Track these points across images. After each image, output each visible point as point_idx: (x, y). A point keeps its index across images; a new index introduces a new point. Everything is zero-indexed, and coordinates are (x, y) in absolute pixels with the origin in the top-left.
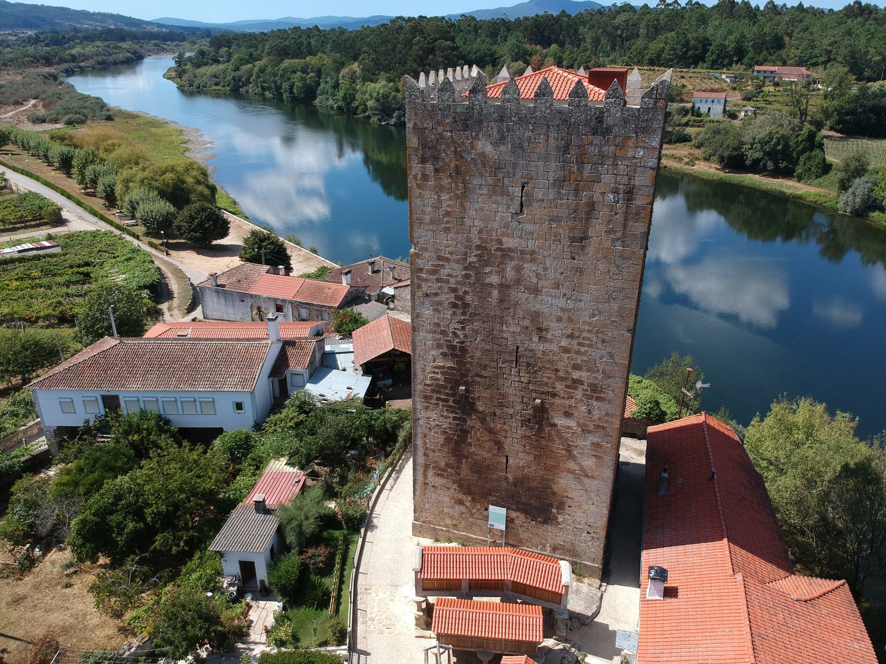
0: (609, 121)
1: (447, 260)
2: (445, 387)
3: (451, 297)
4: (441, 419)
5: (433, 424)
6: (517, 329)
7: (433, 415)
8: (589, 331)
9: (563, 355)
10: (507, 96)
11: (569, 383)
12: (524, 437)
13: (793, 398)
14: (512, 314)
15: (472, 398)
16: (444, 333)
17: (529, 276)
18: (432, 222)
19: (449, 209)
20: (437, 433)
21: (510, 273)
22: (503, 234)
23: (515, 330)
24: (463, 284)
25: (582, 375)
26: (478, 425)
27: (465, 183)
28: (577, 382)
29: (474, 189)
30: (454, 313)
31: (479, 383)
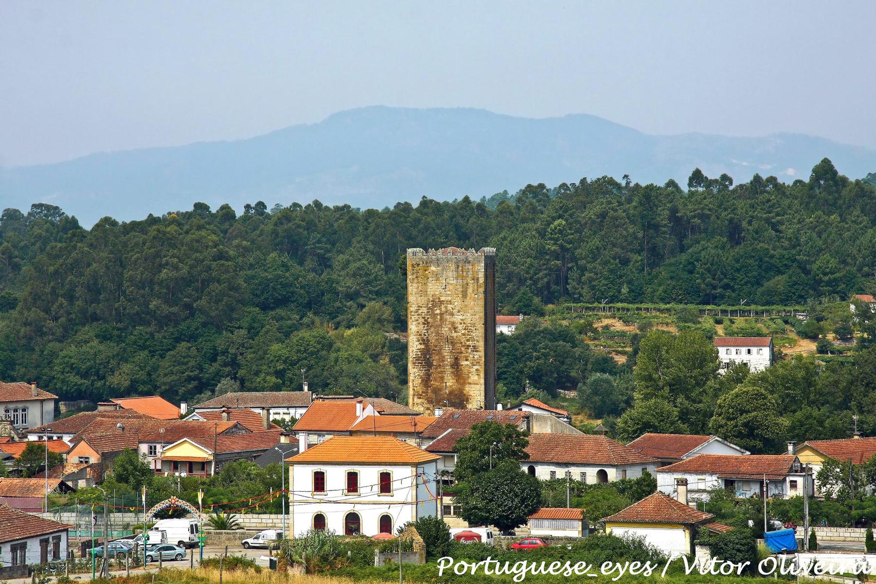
13: (608, 415)
16: (420, 335)
21: (443, 309)
25: (470, 343)
28: (469, 346)
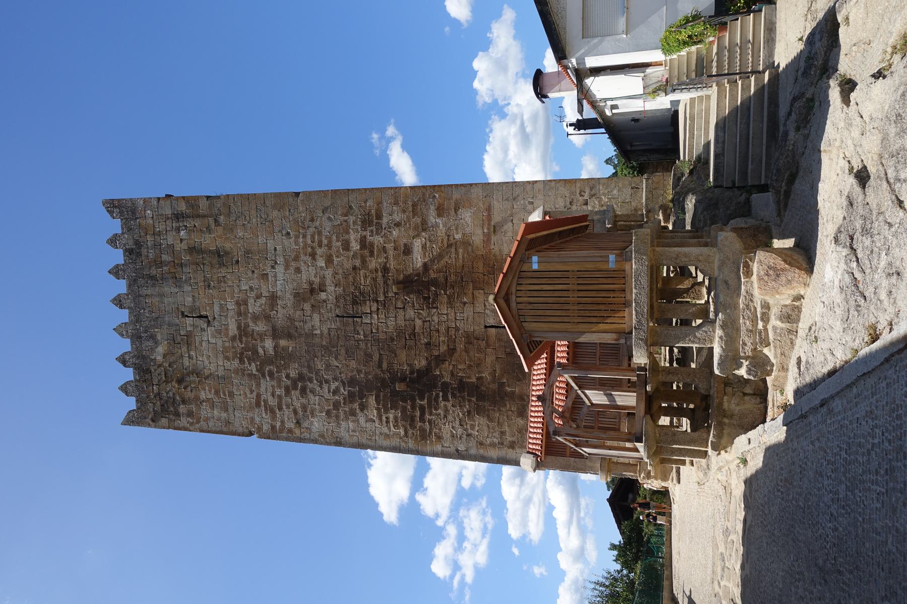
0: (131, 244)
1: (259, 396)
2: (404, 410)
3: (295, 394)
4: (450, 418)
5: (460, 431)
6: (316, 317)
7: (446, 430)
8: (304, 236)
10: (124, 333)
12: (450, 304)
14: (301, 324)
15: (412, 372)
17: (260, 306)
18: (226, 410)
19: (213, 391)
22: (227, 335)
23: (318, 320)
24: (279, 380)
25: (354, 239)
26: (447, 366)
27: (188, 374)
28: (363, 242)
29: (194, 365)
30: (313, 391)
31: (390, 364)
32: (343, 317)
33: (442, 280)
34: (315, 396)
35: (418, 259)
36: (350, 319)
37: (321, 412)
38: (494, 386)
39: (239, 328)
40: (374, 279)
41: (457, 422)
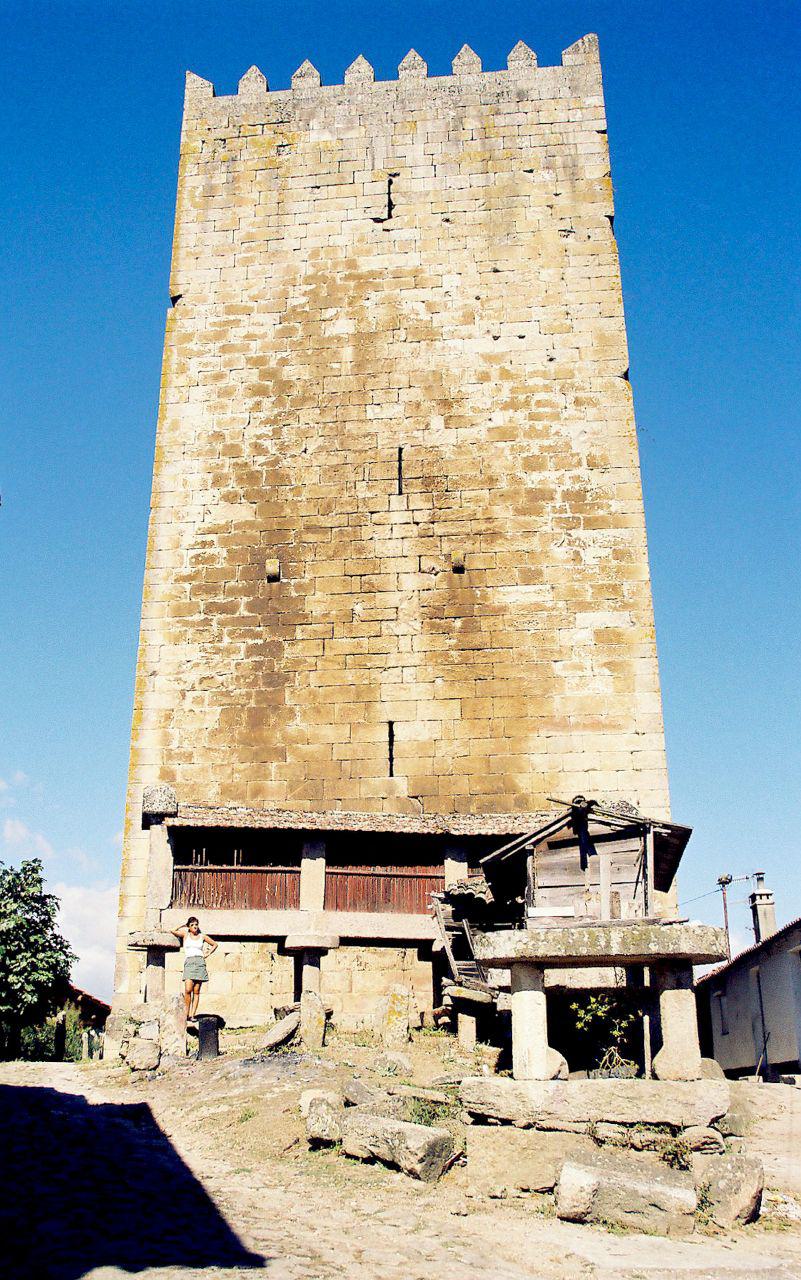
2: (228, 574)
3: (254, 377)
8: (547, 389)
9: (502, 445)
11: (522, 501)
15: (299, 587)
20: (199, 701)
22: (359, 253)
25: (547, 478)
28: (539, 496)
30: (258, 406)
32: (400, 460)
33: (477, 639)
34: (251, 410)
35: (513, 596)
36: (395, 474)
37: (219, 424)
38: (277, 739)
39: (372, 274)
40: (473, 518)
41: (207, 674)
